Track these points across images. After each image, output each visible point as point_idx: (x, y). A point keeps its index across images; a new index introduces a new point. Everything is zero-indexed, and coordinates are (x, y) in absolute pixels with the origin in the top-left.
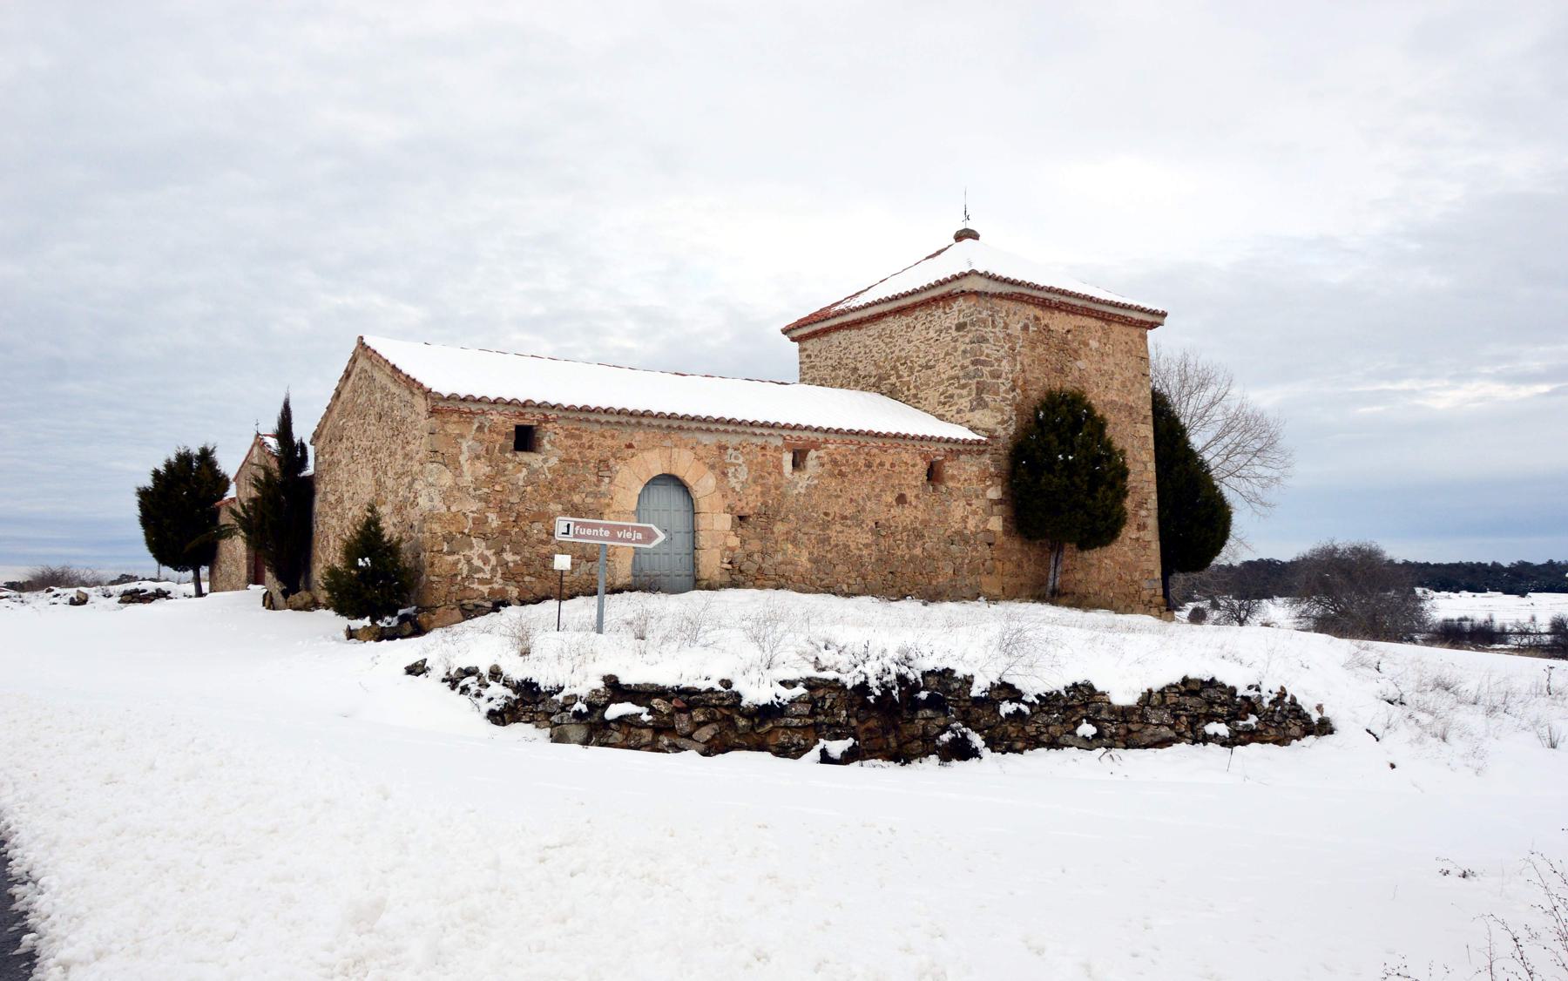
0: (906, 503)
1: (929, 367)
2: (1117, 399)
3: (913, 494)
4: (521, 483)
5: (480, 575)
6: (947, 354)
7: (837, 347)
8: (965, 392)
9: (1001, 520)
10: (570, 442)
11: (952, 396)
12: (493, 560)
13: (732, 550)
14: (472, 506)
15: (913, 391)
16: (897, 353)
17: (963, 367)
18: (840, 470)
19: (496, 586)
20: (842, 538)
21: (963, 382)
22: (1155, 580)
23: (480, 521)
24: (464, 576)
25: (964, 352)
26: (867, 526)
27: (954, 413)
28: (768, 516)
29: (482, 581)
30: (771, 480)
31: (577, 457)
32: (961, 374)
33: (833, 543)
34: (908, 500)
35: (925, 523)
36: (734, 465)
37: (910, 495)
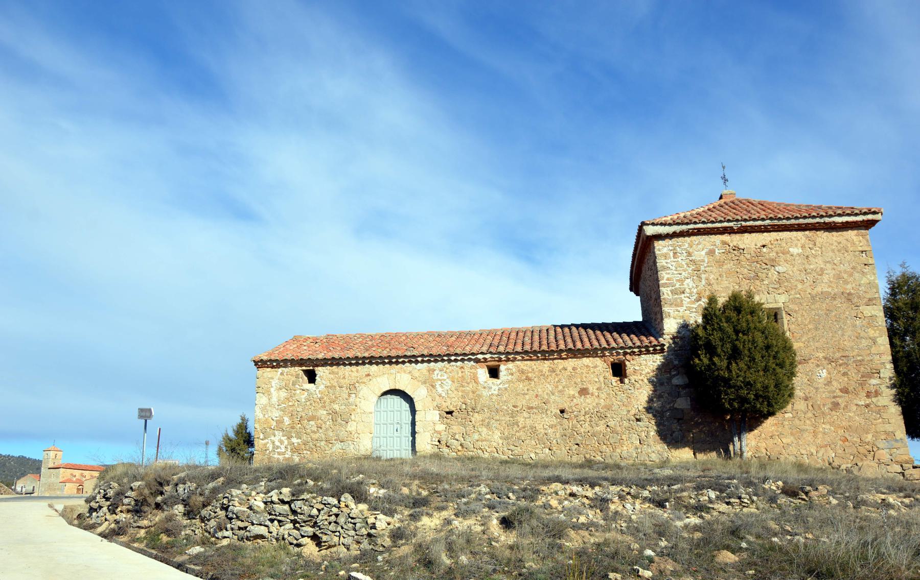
0: (588, 394)
2: (830, 290)
3: (595, 388)
4: (303, 400)
5: (279, 450)
9: (689, 400)
10: (332, 376)
12: (286, 442)
13: (439, 433)
14: (276, 414)
18: (527, 377)
19: (287, 456)
20: (529, 422)
22: (896, 441)
23: (280, 422)
24: (270, 450)
26: (551, 412)
28: (469, 410)
29: (279, 454)
30: (468, 389)
31: (336, 384)
33: (521, 426)
34: (590, 392)
35: (608, 408)
36: (440, 380)
37: (592, 389)
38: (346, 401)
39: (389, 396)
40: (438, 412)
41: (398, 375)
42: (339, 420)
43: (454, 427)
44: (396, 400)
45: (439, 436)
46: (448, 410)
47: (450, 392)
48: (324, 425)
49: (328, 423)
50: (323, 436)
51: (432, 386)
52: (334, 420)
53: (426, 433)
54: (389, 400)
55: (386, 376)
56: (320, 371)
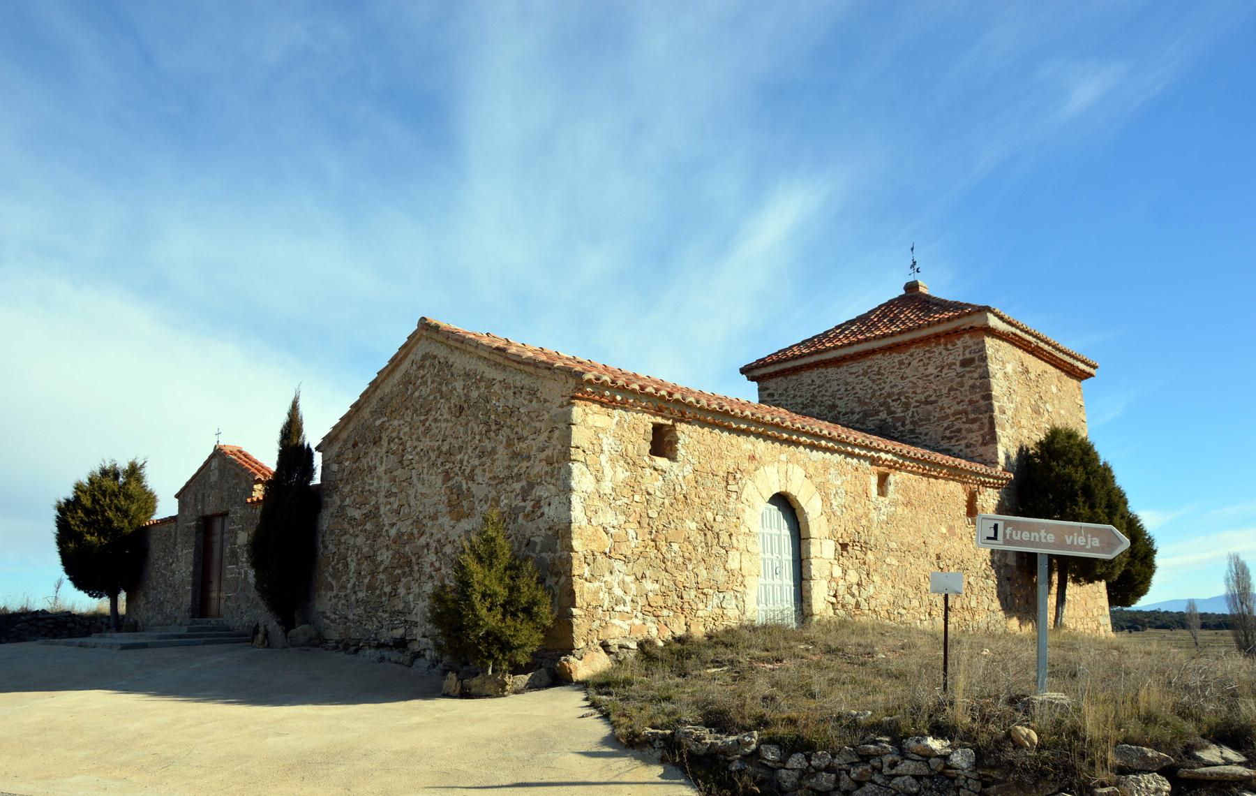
1: (927, 402)
6: (951, 389)
7: (809, 385)
8: (975, 426)
11: (959, 431)
15: (910, 427)
16: (887, 389)
17: (971, 402)
21: (972, 416)
24: (605, 608)
25: (973, 387)
27: (962, 447)
32: (970, 408)
56: (687, 435)
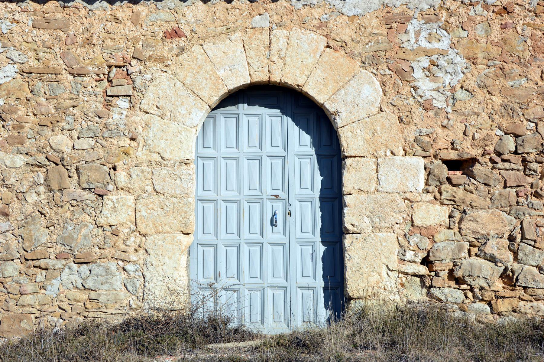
10: (45, 36)
38: (95, 124)
39: (243, 108)
40: (422, 162)
41: (280, 34)
42: (72, 185)
43: (482, 214)
44: (267, 119)
45: (427, 244)
46: (453, 155)
47: (460, 94)
48: (16, 204)
49: (32, 198)
50: (14, 244)
51: (400, 73)
52: (55, 187)
53: (382, 235)
54: (244, 120)
55: (237, 36)
